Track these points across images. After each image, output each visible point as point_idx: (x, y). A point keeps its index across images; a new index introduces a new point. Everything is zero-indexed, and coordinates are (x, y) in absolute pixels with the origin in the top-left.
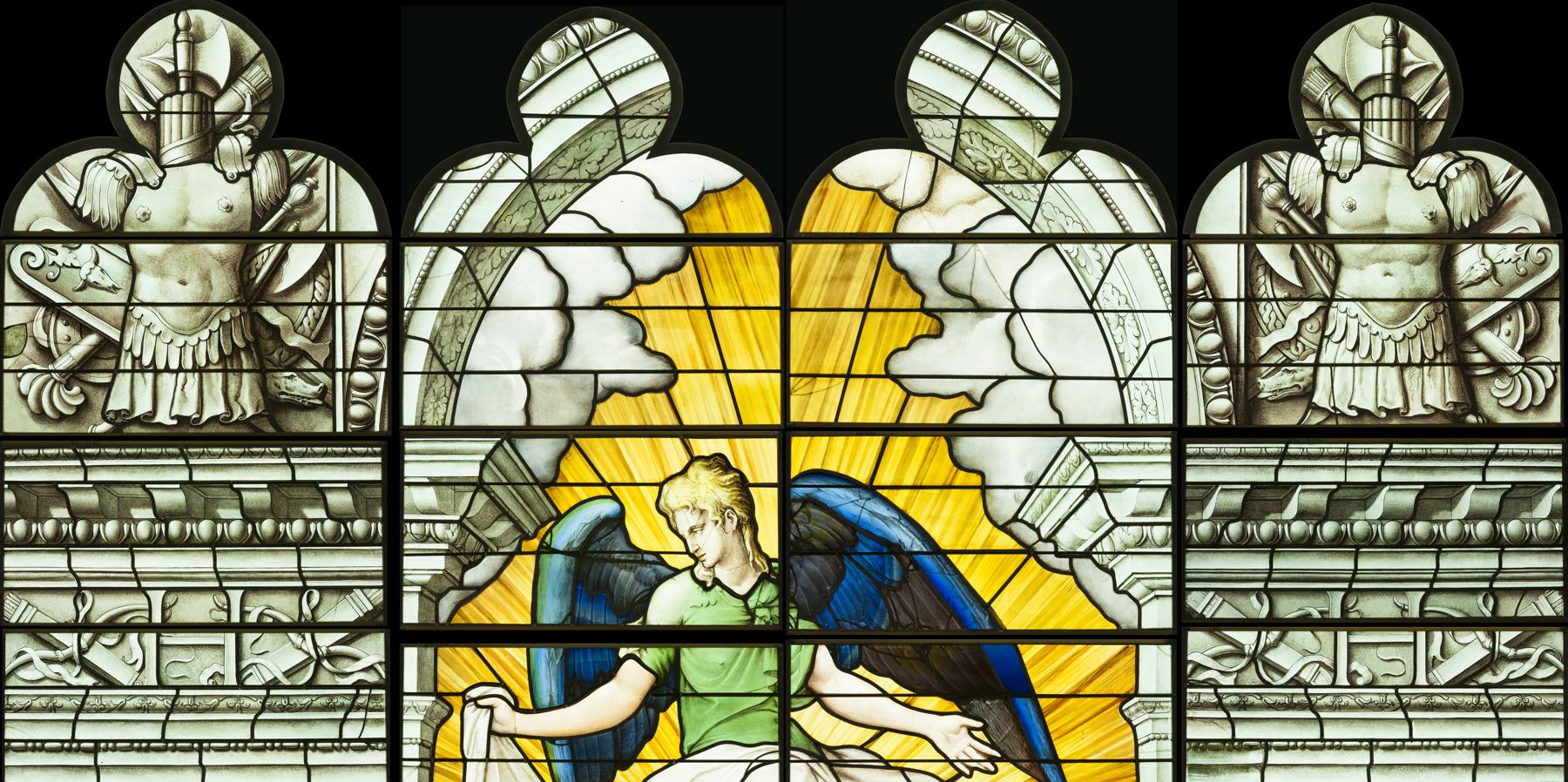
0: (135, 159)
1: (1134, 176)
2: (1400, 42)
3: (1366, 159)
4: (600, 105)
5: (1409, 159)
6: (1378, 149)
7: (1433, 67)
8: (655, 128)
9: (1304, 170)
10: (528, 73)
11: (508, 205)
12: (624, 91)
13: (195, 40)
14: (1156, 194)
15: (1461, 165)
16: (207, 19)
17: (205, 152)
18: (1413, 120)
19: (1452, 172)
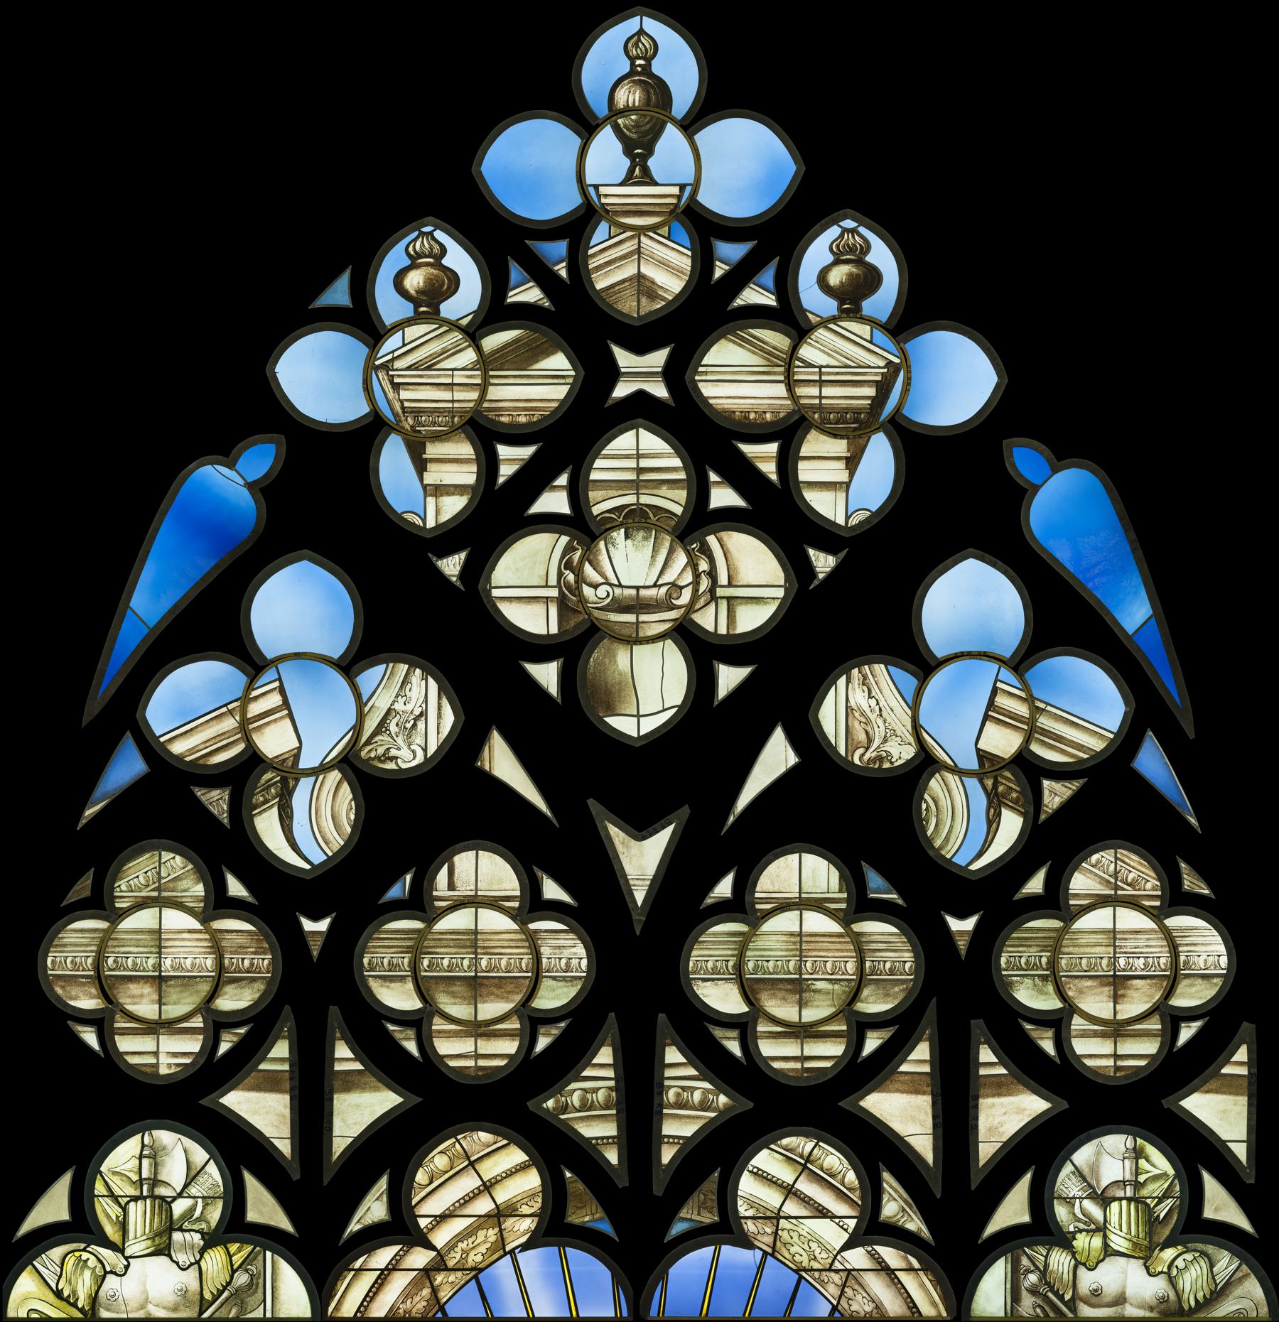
0: (105, 1253)
1: (916, 1264)
2: (1138, 1154)
3: (1108, 1252)
4: (483, 1206)
5: (1144, 1253)
6: (1118, 1243)
7: (1164, 1175)
8: (528, 1224)
9: (1060, 1261)
10: (421, 1177)
11: (407, 1294)
12: (504, 1194)
13: (154, 1155)
14: (937, 1282)
15: (1189, 1257)
16: (165, 1137)
17: (163, 1250)
18: (1151, 1222)
19: (1180, 1263)
